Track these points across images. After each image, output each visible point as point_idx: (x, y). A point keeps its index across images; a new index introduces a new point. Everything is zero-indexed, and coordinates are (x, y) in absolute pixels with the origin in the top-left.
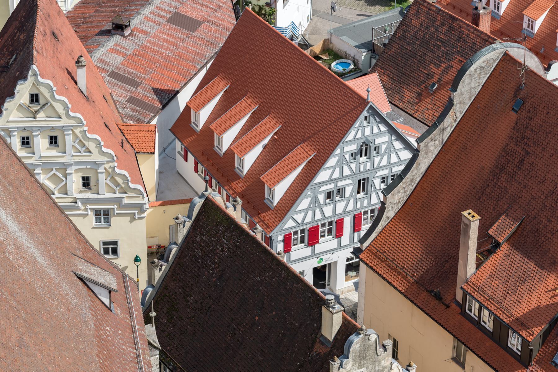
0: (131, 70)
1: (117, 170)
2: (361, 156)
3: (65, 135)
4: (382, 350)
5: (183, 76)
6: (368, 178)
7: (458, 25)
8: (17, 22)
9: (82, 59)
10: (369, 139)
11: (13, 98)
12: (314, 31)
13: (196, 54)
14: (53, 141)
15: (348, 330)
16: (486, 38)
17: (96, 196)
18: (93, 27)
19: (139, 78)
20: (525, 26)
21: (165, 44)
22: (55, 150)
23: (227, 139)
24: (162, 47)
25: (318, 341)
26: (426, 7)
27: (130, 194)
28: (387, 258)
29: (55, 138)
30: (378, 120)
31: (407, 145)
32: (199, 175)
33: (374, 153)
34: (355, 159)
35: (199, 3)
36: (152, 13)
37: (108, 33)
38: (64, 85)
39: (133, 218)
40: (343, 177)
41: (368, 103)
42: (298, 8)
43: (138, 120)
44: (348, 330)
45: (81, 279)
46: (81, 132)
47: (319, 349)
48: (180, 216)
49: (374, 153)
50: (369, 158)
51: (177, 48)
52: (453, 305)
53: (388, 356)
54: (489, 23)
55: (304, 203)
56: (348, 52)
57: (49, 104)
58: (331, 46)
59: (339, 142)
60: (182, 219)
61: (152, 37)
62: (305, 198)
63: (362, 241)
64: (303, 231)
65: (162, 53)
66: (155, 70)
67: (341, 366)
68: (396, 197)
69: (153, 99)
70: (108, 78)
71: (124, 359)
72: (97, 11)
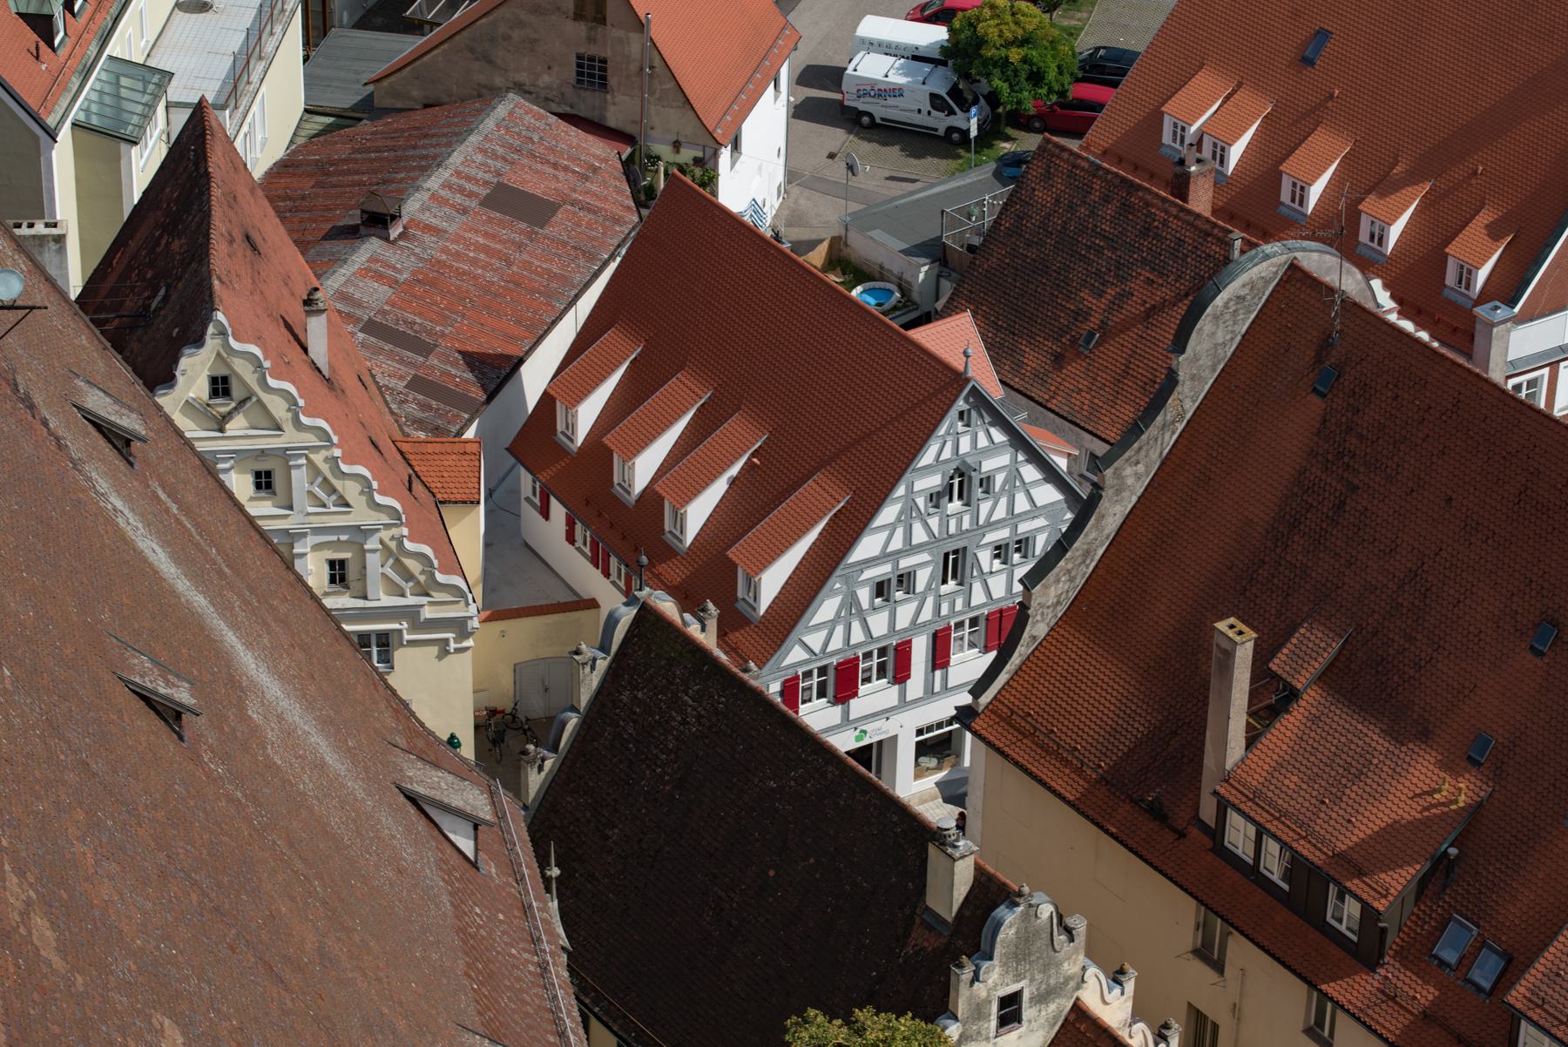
0: (410, 317)
1: (408, 545)
2: (951, 500)
3: (290, 468)
4: (1063, 938)
5: (527, 327)
6: (965, 549)
7: (1141, 199)
8: (159, 213)
9: (318, 295)
10: (969, 460)
11: (172, 387)
12: (791, 214)
13: (553, 277)
14: (264, 482)
15: (990, 894)
16: (1208, 227)
17: (360, 603)
18: (315, 221)
19: (429, 333)
20: (1285, 197)
21: (482, 256)
22: (269, 503)
23: (645, 467)
24: (474, 262)
25: (918, 920)
26: (1067, 161)
27: (438, 596)
28: (1036, 729)
29: (268, 474)
30: (987, 419)
31: (1051, 474)
32: (578, 549)
33: (978, 492)
34: (937, 506)
35: (548, 162)
36: (447, 185)
37: (352, 233)
38: (282, 355)
39: (444, 652)
40: (910, 548)
41: (968, 380)
42: (760, 167)
43: (437, 430)
44: (990, 894)
45: (413, 799)
46: (326, 460)
47: (921, 939)
48: (583, 647)
49: (978, 492)
50: (967, 504)
51: (510, 264)
52: (1194, 832)
53: (1076, 951)
54: (1210, 194)
55: (827, 608)
56: (887, 266)
57: (254, 399)
58: (845, 252)
59: (904, 471)
60: (588, 651)
61: (453, 242)
62: (829, 596)
63: (978, 688)
64: (823, 671)
65: (475, 277)
66: (463, 316)
67: (976, 978)
68: (1053, 592)
69: (466, 381)
70: (361, 335)
71: (518, 979)
72: (318, 184)
